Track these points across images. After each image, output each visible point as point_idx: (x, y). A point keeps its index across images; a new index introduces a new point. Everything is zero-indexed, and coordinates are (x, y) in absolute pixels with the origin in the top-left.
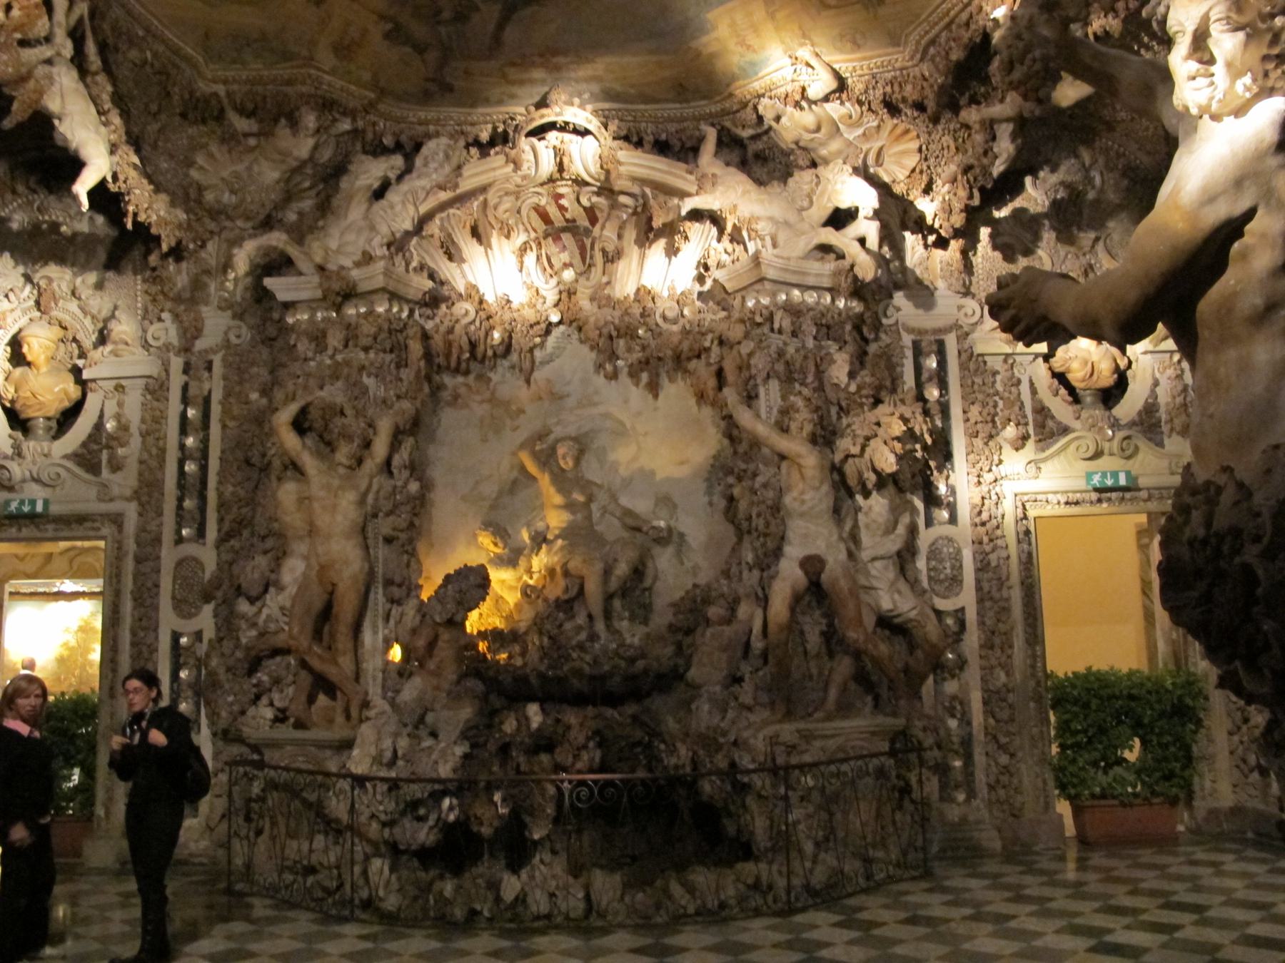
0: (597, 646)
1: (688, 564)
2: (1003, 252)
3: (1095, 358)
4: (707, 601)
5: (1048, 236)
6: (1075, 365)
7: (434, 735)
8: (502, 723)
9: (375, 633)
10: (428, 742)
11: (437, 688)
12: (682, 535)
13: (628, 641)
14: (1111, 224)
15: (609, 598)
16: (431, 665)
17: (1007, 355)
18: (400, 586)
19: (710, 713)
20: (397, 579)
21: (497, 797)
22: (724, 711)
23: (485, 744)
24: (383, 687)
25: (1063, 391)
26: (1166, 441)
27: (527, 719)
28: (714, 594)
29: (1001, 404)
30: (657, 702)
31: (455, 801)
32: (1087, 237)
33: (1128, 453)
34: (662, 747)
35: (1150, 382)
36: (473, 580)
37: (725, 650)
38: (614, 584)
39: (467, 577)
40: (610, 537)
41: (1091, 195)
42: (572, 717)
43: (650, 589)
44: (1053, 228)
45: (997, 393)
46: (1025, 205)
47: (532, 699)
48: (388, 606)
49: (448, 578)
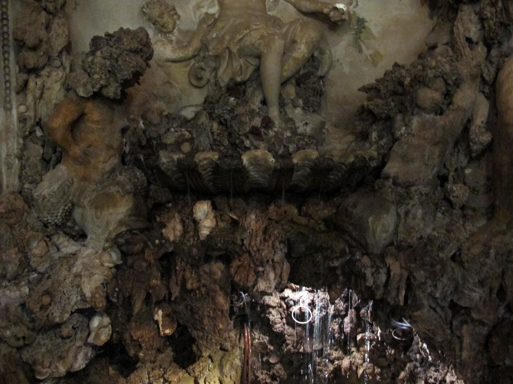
0: (271, 133)
1: (367, 52)
4: (420, 81)
7: (81, 236)
8: (163, 226)
9: (8, 110)
10: (69, 247)
11: (85, 179)
12: (361, 22)
13: (300, 130)
15: (284, 84)
16: (76, 150)
18: (34, 49)
19: (423, 219)
20: (31, 41)
21: (159, 315)
22: (435, 216)
23: (143, 252)
24: (20, 177)
27: (196, 222)
28: (430, 73)
30: (357, 204)
31: (107, 320)
34: (366, 260)
36: (127, 43)
37: (436, 144)
38: (290, 68)
39: (119, 40)
40: (286, 19)
42: (252, 221)
43: (322, 78)
47: (203, 194)
48: (25, 76)
49: (96, 41)
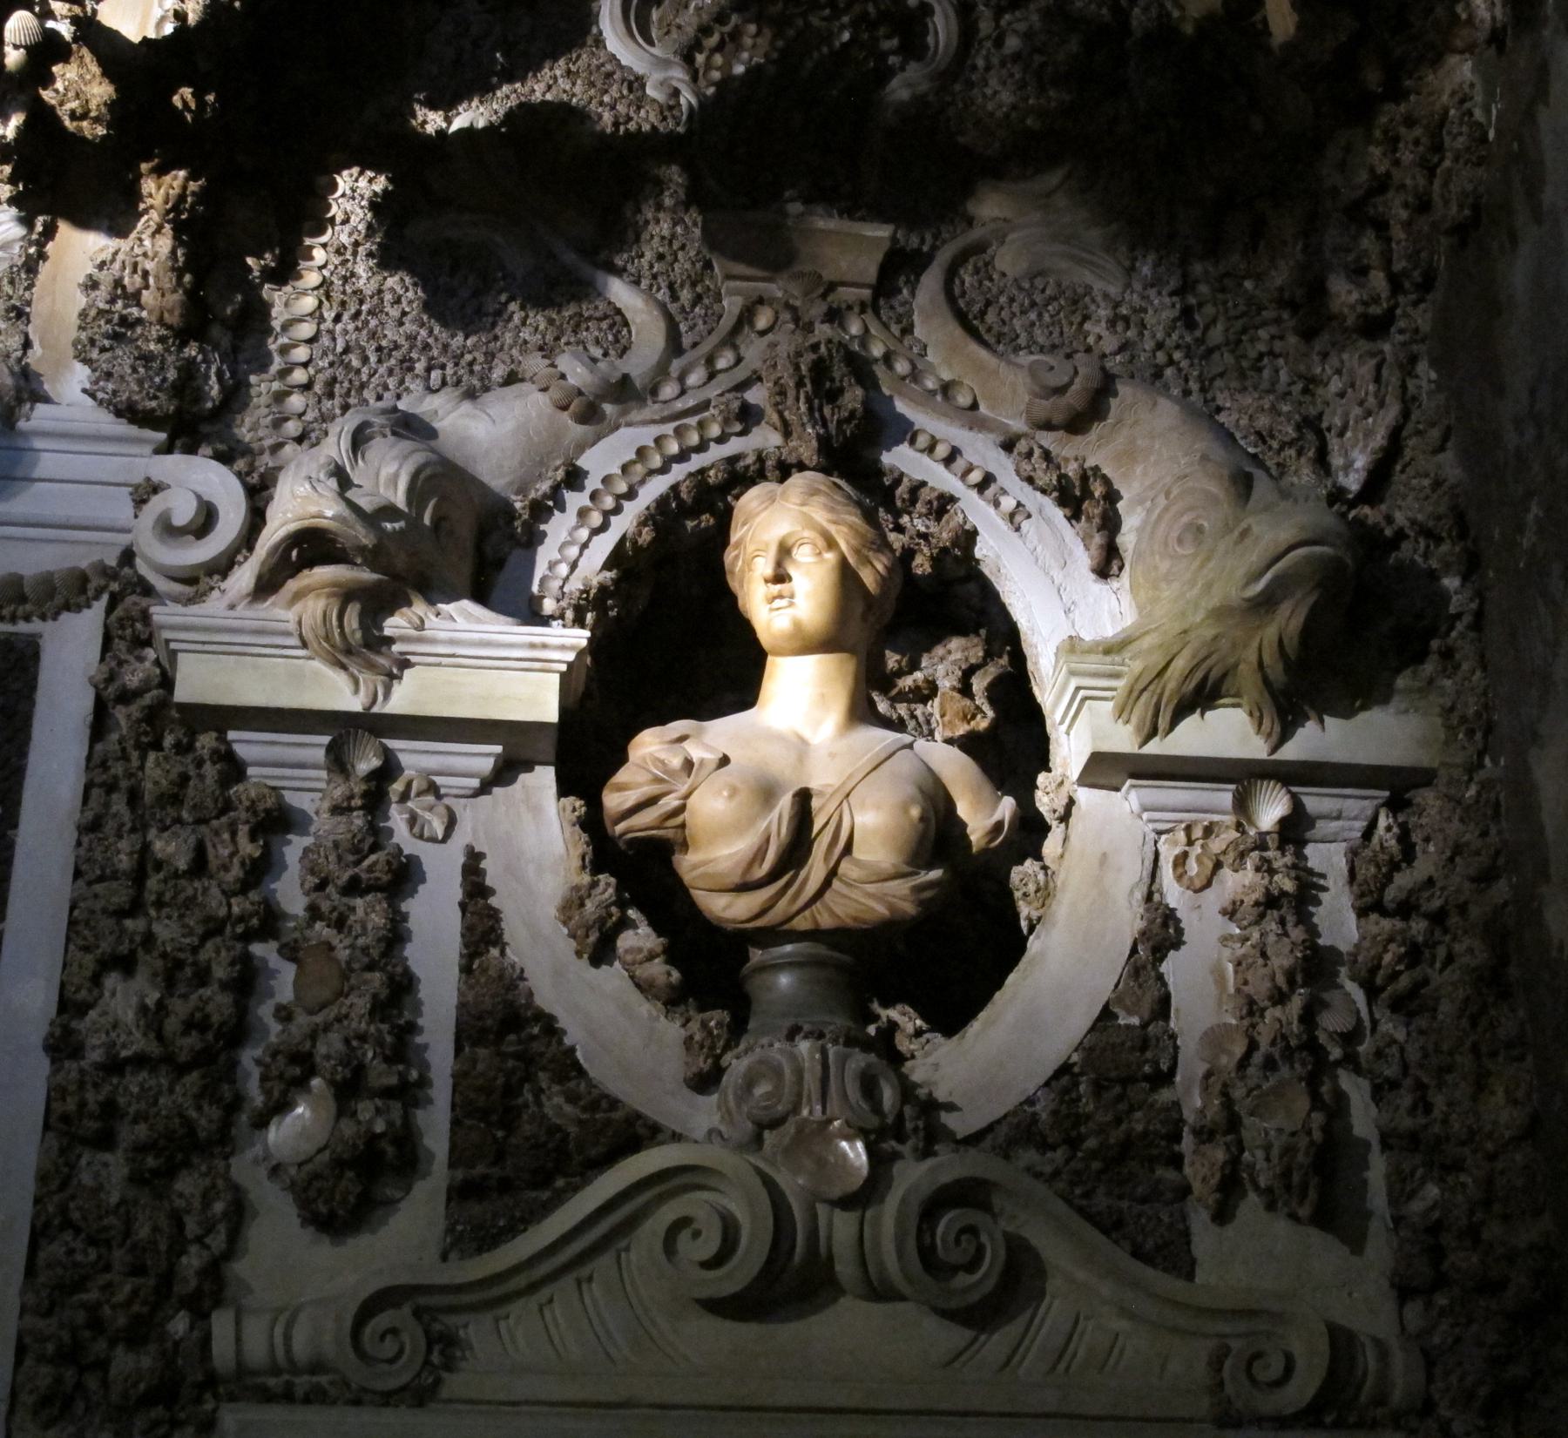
2: (425, 279)
3: (822, 778)
5: (667, 229)
6: (711, 805)
14: (990, 207)
17: (344, 731)
25: (640, 937)
26: (1204, 1237)
29: (284, 981)
32: (851, 247)
33: (979, 1282)
35: (1128, 921)
41: (905, 85)
44: (695, 197)
45: (269, 922)
46: (578, 93)
